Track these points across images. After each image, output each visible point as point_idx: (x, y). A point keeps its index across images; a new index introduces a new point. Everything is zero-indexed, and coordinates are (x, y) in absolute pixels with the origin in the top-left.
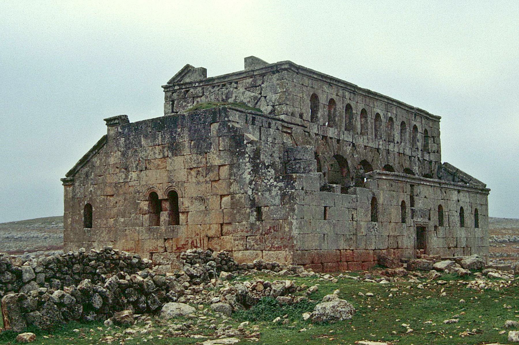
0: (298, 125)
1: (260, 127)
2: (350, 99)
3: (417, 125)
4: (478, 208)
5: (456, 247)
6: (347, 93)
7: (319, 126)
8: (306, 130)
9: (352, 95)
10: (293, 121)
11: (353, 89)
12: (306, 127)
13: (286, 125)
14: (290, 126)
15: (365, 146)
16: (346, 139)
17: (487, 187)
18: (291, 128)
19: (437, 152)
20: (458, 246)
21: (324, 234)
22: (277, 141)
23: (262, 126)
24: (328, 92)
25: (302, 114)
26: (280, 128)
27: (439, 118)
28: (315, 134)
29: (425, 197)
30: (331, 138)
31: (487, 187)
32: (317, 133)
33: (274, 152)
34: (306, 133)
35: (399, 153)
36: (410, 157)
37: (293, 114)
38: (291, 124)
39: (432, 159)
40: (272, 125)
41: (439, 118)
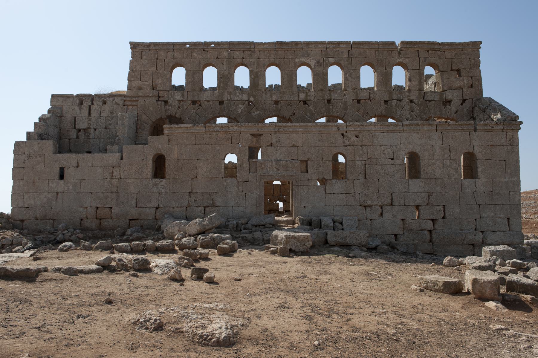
0: (147, 96)
1: (90, 106)
2: (243, 58)
3: (406, 61)
4: (477, 150)
5: (392, 204)
6: (237, 53)
7: (185, 94)
8: (161, 99)
9: (248, 53)
10: (140, 94)
11: (248, 47)
12: (163, 97)
13: (128, 99)
14: (137, 99)
15: (277, 103)
16: (236, 98)
17: (519, 120)
18: (137, 101)
19: (471, 87)
20: (395, 203)
21: (57, 194)
22: (115, 114)
23: (93, 104)
24: (201, 57)
25: (156, 85)
26: (121, 103)
27: (477, 45)
28: (180, 101)
29: (294, 146)
30: (209, 101)
31: (519, 120)
32: (181, 99)
33: (110, 124)
34: (159, 102)
35: (359, 101)
36: (386, 102)
37: (140, 89)
38: (139, 97)
39: (449, 97)
40: (108, 102)
41: (477, 45)
